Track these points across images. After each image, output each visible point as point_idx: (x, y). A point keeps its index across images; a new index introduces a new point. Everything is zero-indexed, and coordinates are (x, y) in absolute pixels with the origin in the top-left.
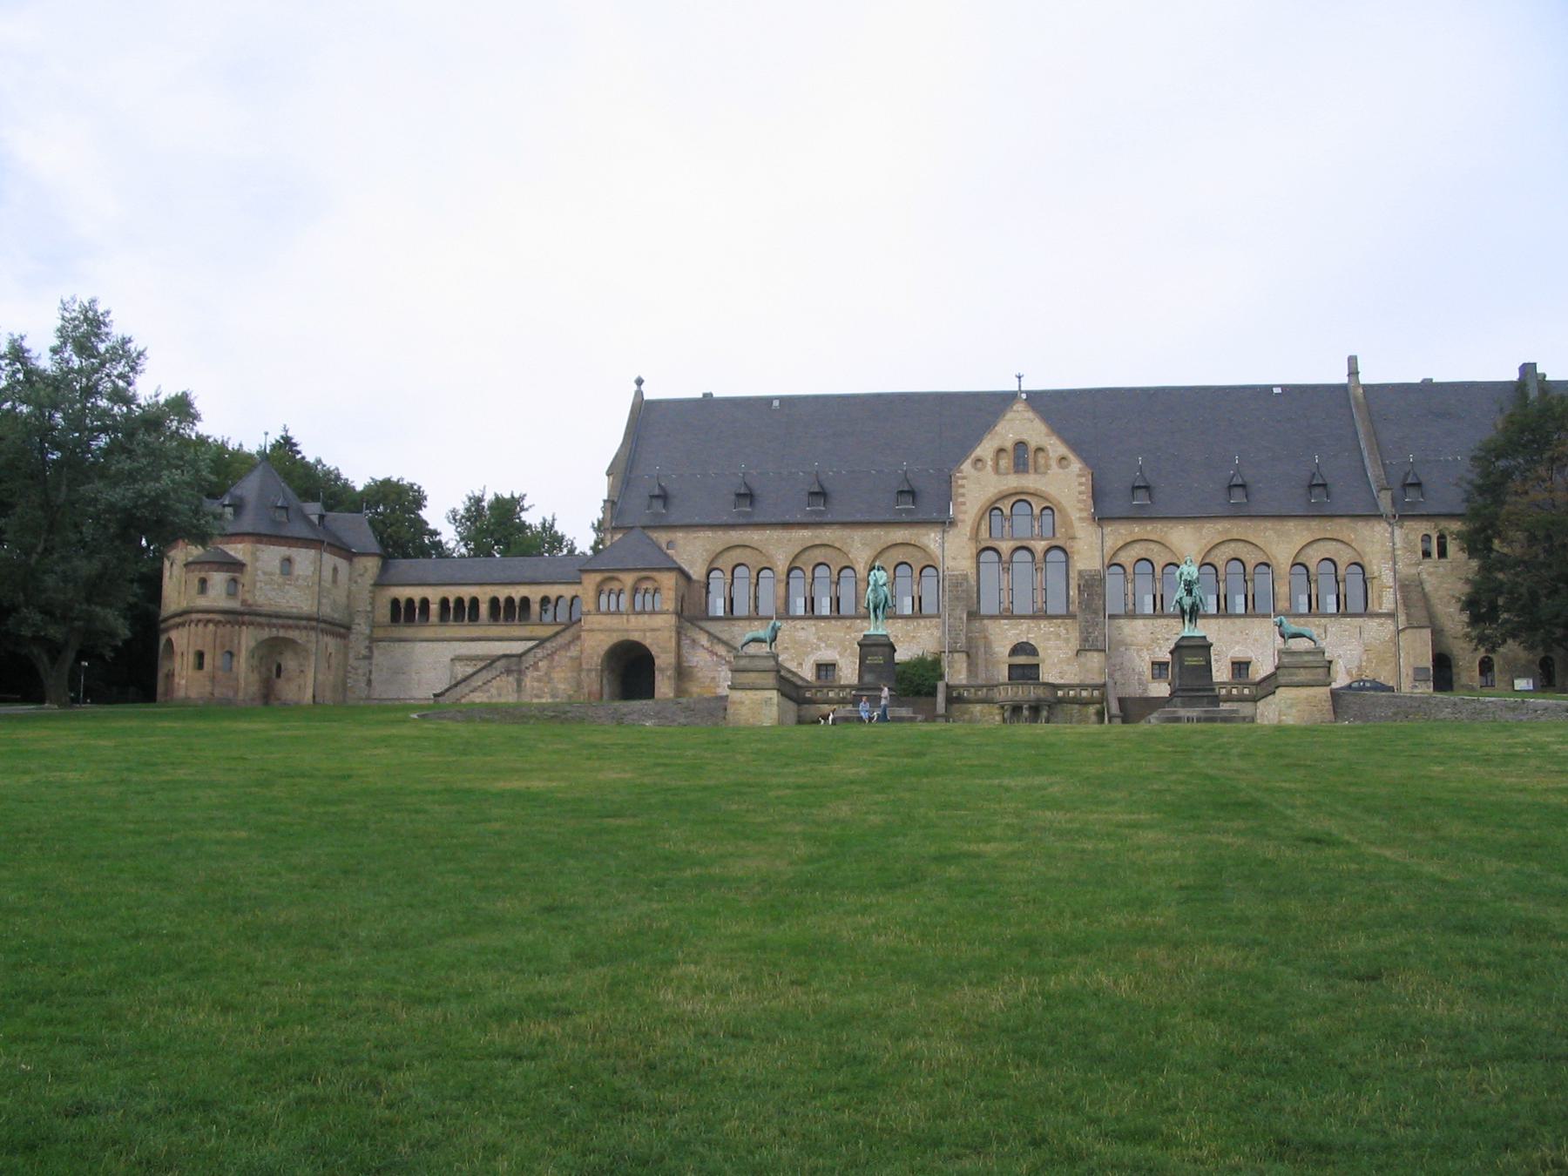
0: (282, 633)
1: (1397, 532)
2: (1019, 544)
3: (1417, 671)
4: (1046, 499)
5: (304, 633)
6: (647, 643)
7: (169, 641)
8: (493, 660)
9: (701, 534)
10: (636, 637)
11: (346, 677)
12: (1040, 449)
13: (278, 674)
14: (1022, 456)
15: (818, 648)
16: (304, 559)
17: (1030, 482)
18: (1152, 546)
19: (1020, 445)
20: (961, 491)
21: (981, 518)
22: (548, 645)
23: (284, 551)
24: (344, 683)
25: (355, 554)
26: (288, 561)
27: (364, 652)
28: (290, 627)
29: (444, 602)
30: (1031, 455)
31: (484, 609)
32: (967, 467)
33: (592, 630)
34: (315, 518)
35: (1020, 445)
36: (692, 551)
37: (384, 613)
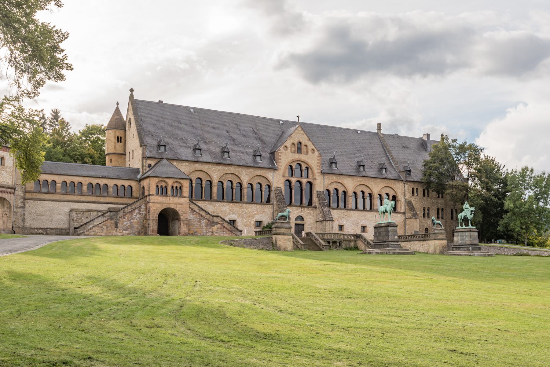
1: (406, 186)
4: (307, 164)
9: (184, 164)
10: (173, 206)
14: (299, 148)
15: (230, 214)
17: (302, 157)
18: (339, 184)
20: (280, 158)
22: (130, 208)
27: (21, 205)
31: (85, 188)
32: (282, 148)
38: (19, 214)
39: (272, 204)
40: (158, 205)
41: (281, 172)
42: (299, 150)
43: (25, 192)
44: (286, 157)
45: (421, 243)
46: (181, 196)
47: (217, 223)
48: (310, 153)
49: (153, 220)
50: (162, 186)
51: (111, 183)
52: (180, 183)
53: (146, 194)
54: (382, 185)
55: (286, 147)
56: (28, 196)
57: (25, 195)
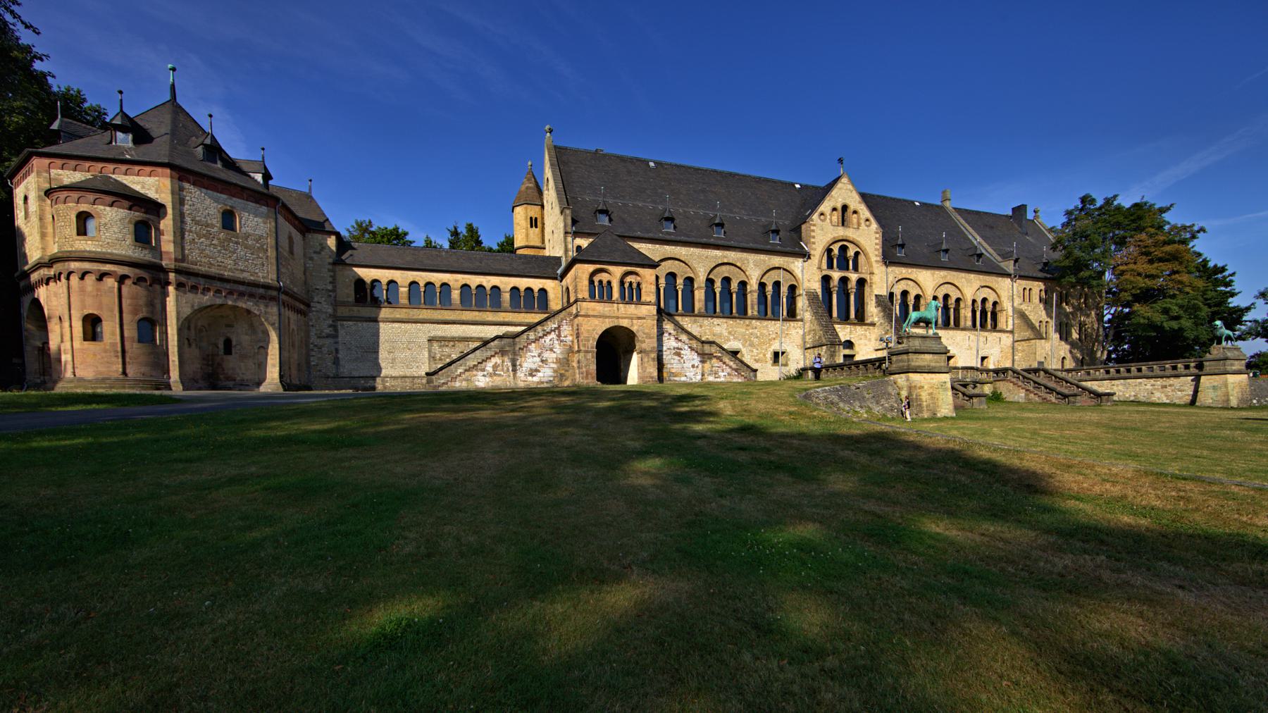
10: (625, 323)
12: (855, 212)
15: (729, 340)
19: (845, 208)
22: (539, 328)
24: (308, 362)
31: (456, 295)
32: (815, 216)
33: (587, 316)
37: (348, 293)
38: (325, 350)
39: (802, 320)
40: (596, 321)
41: (815, 260)
43: (336, 304)
44: (822, 231)
45: (1159, 382)
46: (639, 302)
47: (710, 356)
48: (863, 226)
49: (587, 352)
50: (601, 282)
51: (506, 283)
52: (636, 274)
53: (572, 300)
54: (977, 284)
55: (822, 214)
56: (342, 311)
57: (335, 310)
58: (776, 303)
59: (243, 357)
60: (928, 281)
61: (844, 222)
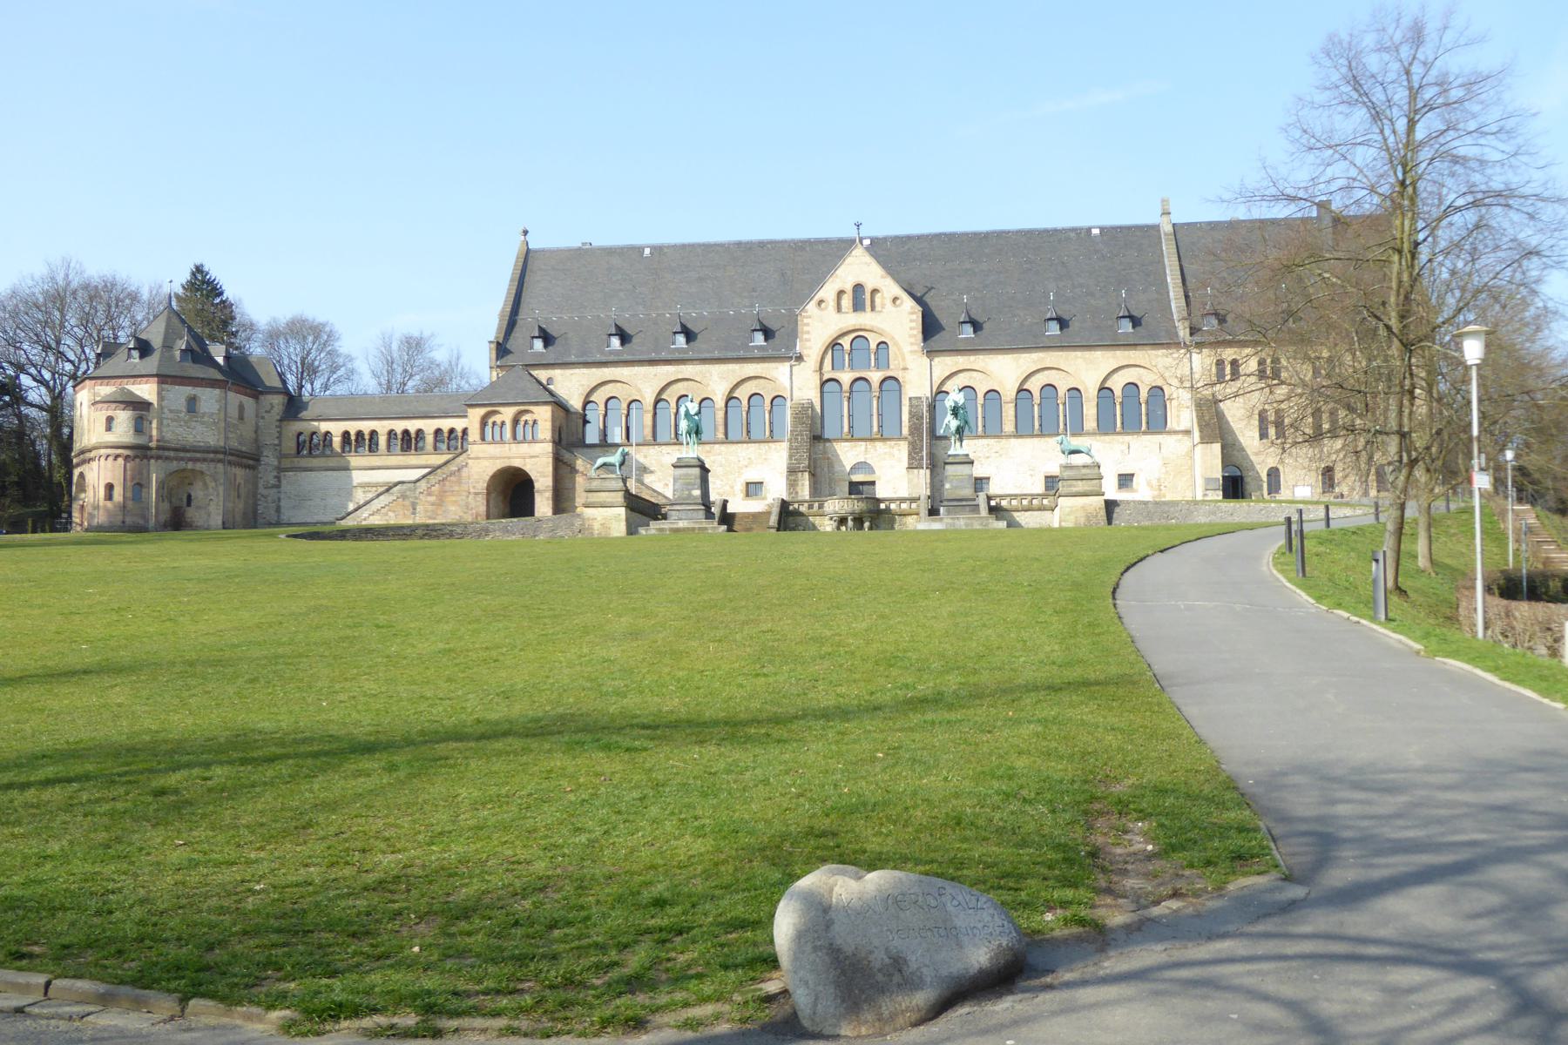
0: (190, 465)
2: (858, 375)
3: (1208, 481)
5: (212, 465)
6: (527, 469)
7: (82, 475)
8: (389, 488)
11: (255, 505)
12: (875, 291)
13: (189, 504)
14: (860, 297)
16: (209, 399)
17: (864, 319)
19: (858, 288)
21: (825, 352)
23: (189, 390)
25: (261, 393)
26: (192, 402)
28: (195, 460)
29: (346, 435)
30: (868, 296)
32: (811, 307)
34: (220, 360)
35: (858, 288)
36: (571, 385)
42: (858, 306)
58: (743, 420)
59: (199, 508)
60: (1003, 371)
61: (858, 306)
